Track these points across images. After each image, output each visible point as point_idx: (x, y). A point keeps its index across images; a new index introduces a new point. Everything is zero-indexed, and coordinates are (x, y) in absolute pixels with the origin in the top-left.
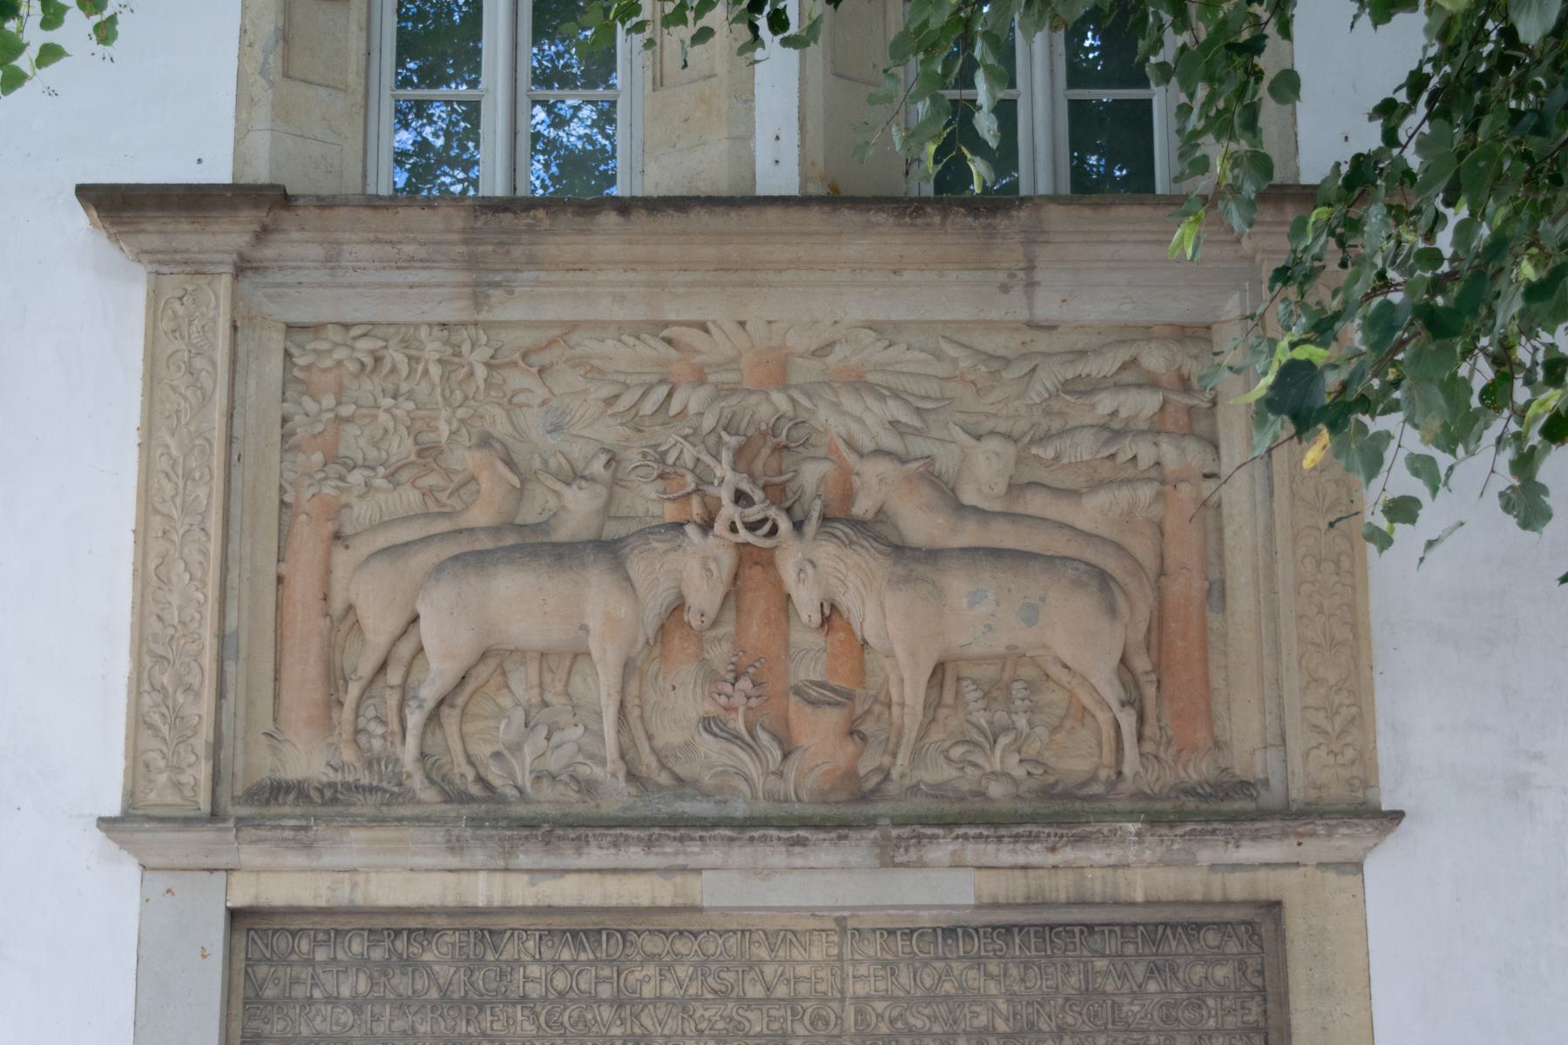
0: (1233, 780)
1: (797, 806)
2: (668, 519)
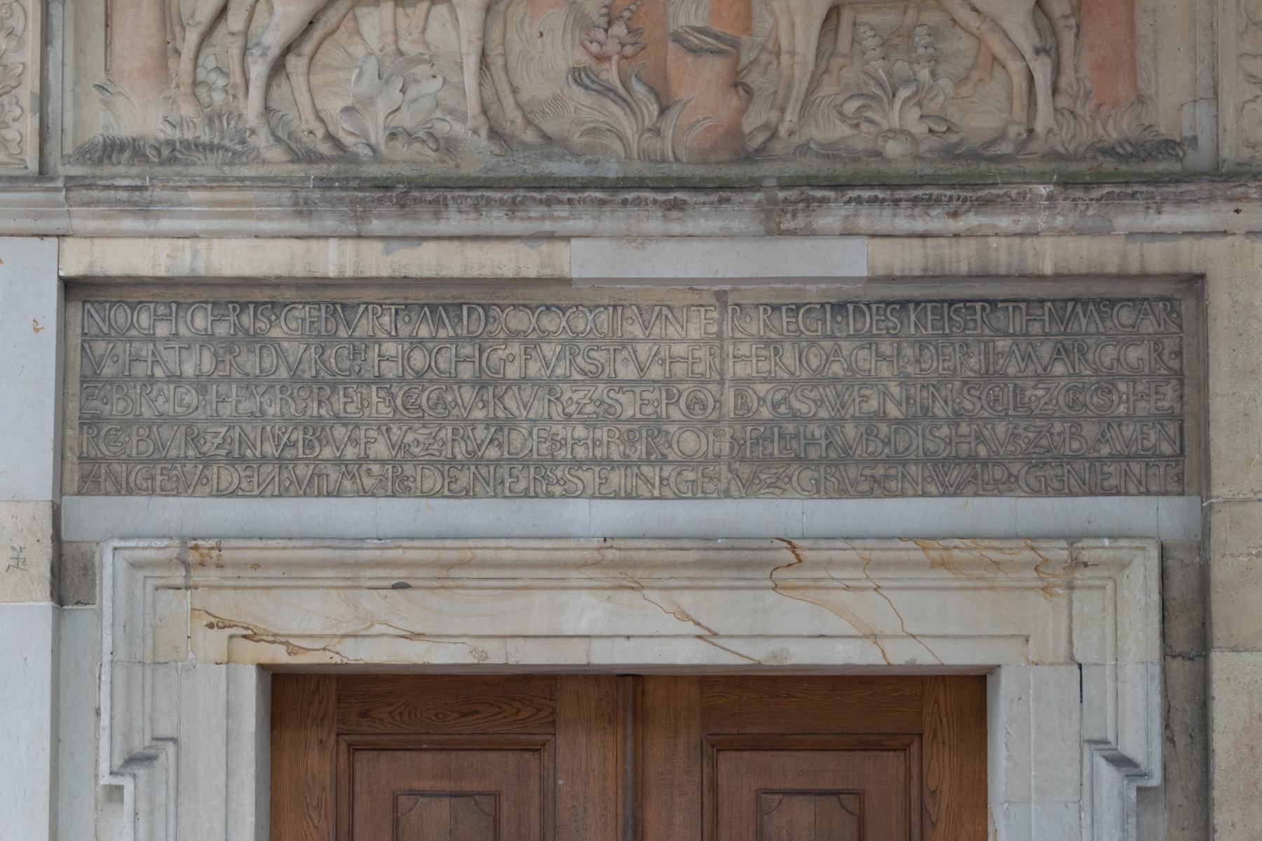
0: (1157, 139)
1: (675, 166)
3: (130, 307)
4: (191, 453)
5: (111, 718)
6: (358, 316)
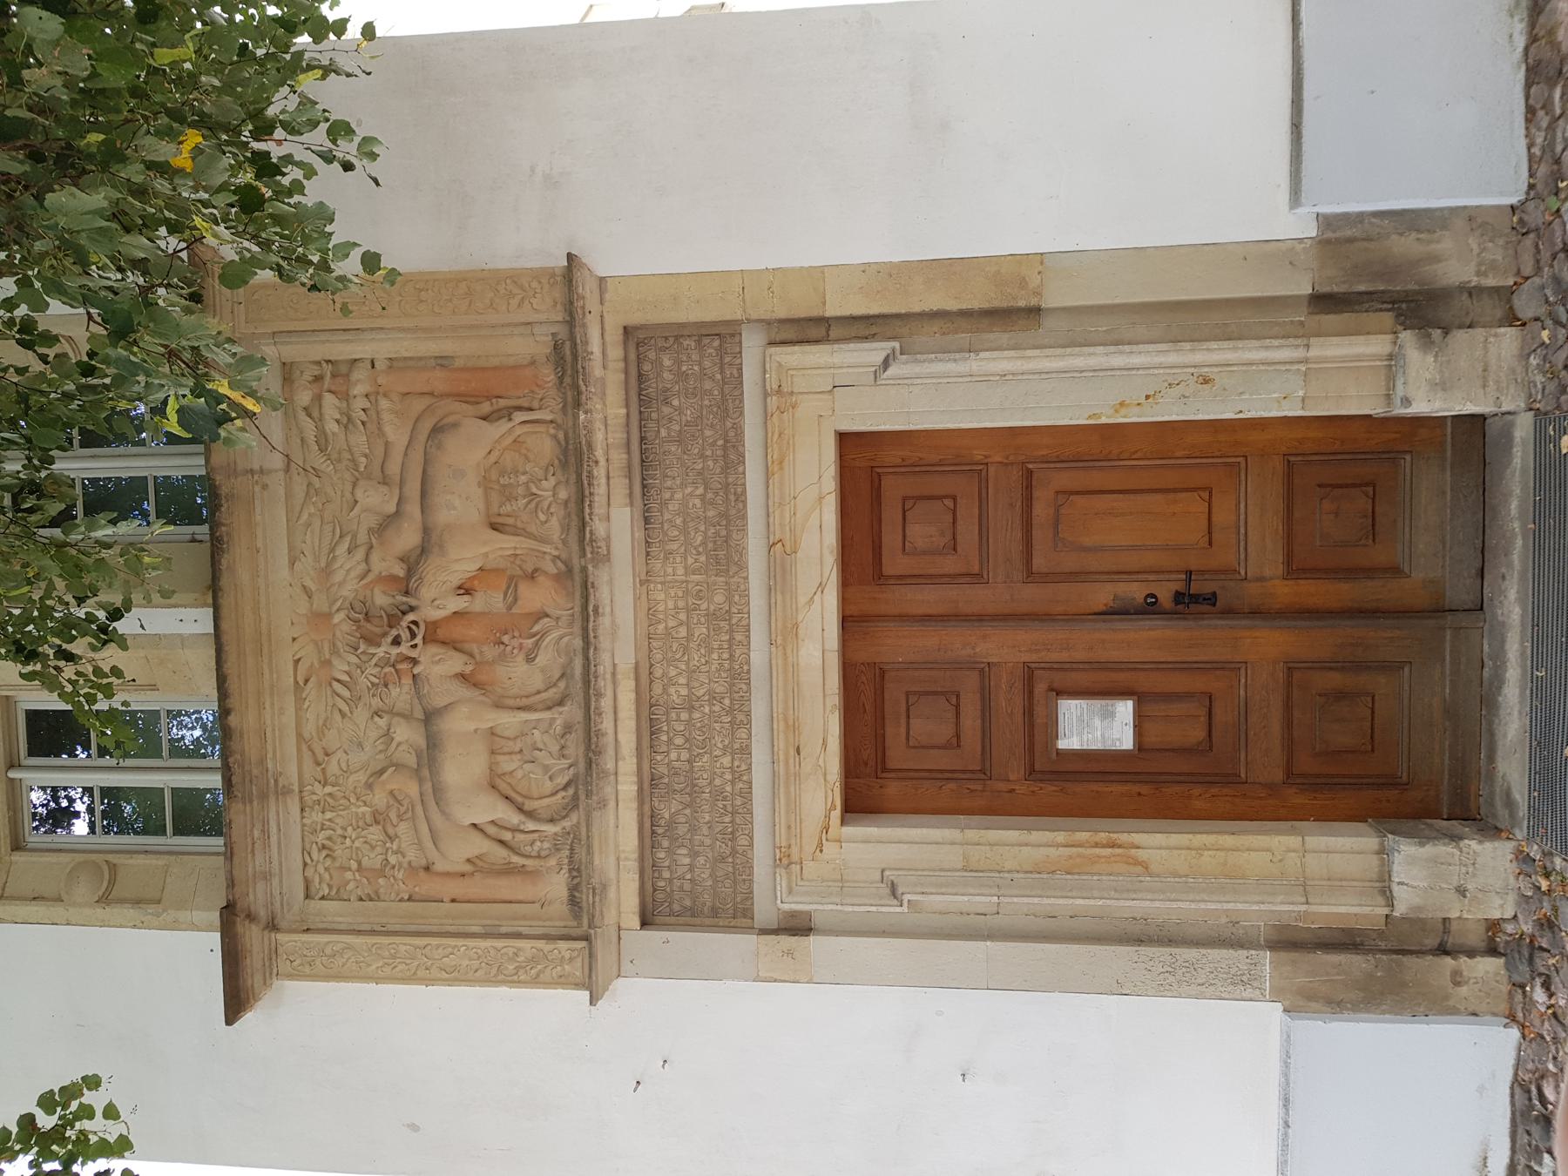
1: (576, 609)
2: (411, 682)
4: (730, 860)
5: (872, 905)
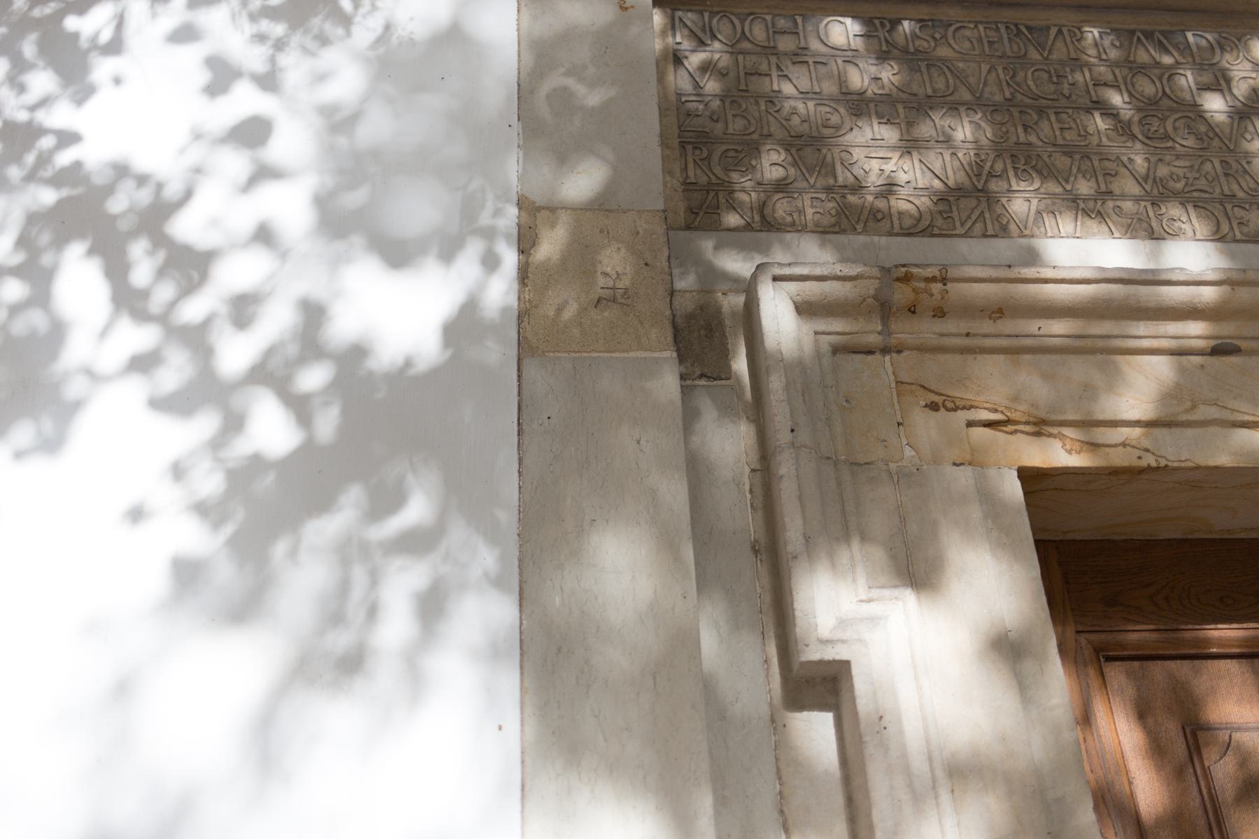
3: (739, 19)
6: (1052, 38)
